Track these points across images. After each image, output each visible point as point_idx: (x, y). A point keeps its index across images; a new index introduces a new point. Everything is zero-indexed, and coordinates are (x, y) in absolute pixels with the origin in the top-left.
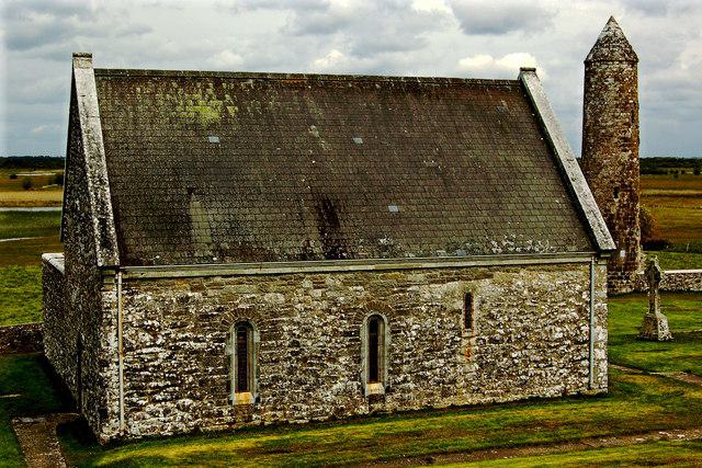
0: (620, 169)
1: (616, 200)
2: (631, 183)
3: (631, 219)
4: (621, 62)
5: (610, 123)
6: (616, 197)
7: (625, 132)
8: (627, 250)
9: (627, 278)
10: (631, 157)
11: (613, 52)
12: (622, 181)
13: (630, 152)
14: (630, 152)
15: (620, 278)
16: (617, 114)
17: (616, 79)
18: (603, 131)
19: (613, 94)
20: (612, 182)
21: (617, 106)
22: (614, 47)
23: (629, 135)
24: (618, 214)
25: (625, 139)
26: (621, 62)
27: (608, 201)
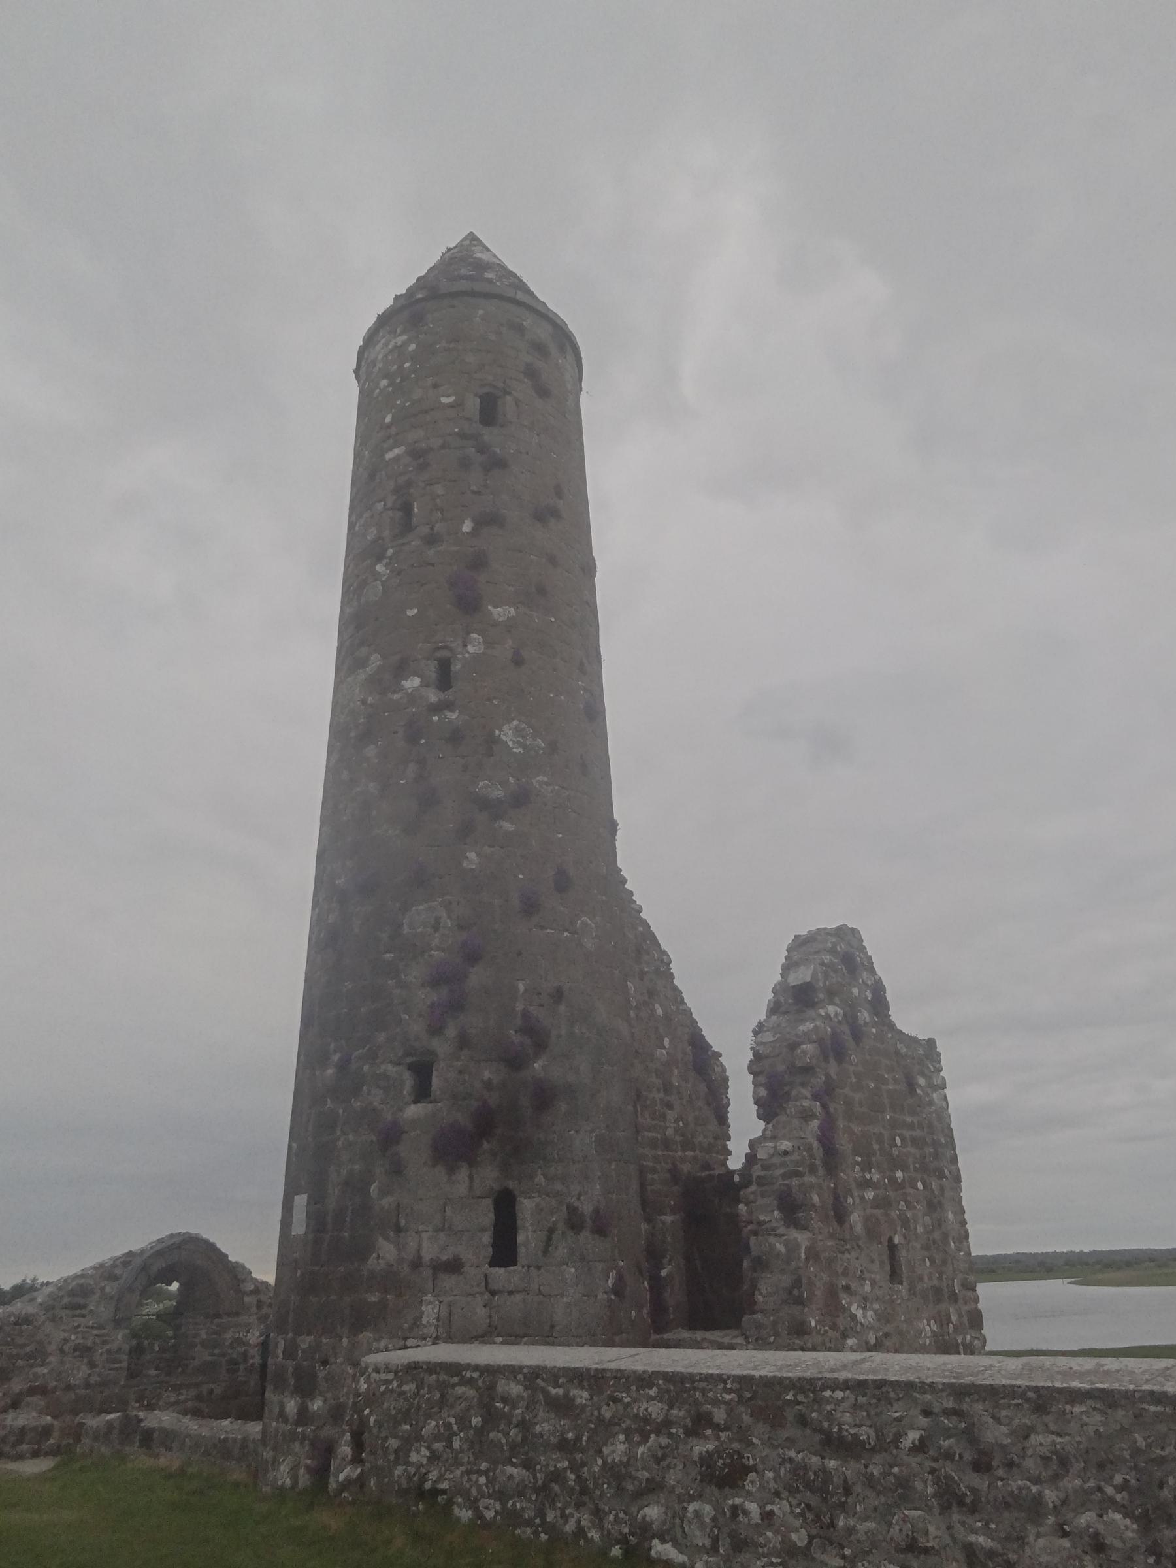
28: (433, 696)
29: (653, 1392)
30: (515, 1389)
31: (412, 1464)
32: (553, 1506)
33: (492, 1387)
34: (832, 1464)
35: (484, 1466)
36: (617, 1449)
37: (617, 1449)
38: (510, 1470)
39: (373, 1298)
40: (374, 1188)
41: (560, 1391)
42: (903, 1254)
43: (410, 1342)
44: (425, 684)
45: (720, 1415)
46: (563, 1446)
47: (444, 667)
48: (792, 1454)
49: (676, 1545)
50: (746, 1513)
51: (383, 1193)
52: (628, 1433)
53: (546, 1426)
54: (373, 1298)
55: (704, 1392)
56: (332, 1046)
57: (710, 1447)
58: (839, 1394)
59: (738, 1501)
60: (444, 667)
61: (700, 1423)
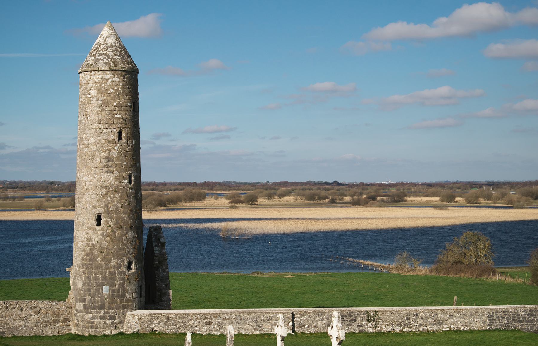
0: (104, 191)
1: (99, 228)
2: (117, 208)
5: (92, 141)
7: (110, 150)
8: (111, 285)
9: (112, 318)
10: (116, 178)
11: (98, 60)
12: (106, 206)
14: (116, 174)
15: (101, 318)
16: (100, 131)
17: (99, 91)
18: (86, 150)
19: (96, 109)
20: (95, 207)
21: (100, 121)
22: (100, 55)
24: (101, 245)
27: (90, 228)
29: (198, 315)
30: (173, 316)
31: (151, 327)
32: (180, 330)
33: (169, 316)
34: (223, 321)
35: (166, 326)
36: (192, 322)
37: (192, 322)
38: (172, 326)
39: (126, 304)
40: (125, 285)
41: (182, 316)
43: (132, 310)
45: (209, 317)
46: (183, 322)
48: (218, 321)
49: (201, 331)
50: (211, 327)
51: (127, 287)
52: (194, 320)
53: (180, 320)
54: (126, 304)
55: (206, 315)
56: (112, 258)
57: (207, 321)
58: (226, 314)
59: (210, 326)
61: (206, 318)
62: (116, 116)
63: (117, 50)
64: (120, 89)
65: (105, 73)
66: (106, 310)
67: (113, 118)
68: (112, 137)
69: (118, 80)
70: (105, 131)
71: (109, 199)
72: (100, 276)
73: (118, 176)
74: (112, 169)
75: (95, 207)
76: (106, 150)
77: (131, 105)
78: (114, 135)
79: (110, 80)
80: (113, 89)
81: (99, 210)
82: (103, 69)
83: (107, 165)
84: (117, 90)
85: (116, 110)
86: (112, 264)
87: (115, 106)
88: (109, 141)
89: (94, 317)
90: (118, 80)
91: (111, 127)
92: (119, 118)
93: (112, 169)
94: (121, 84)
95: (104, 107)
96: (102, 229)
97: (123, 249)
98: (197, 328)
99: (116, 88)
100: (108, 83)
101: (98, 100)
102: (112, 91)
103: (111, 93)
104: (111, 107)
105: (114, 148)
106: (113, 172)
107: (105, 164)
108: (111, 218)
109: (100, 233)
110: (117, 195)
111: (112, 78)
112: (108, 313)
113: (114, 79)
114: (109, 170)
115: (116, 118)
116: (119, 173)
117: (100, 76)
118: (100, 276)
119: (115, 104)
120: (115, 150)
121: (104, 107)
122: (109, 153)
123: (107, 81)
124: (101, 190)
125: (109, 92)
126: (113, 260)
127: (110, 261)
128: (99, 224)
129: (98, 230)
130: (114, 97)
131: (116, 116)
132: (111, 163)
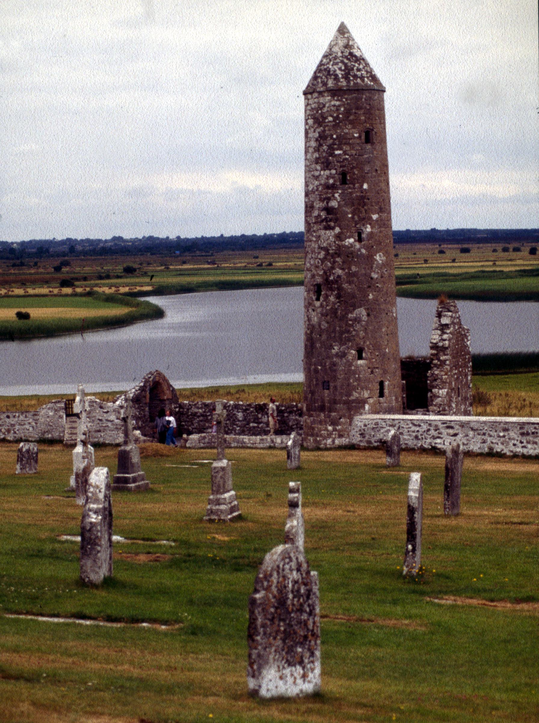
0: (322, 255)
1: (318, 304)
2: (339, 277)
3: (342, 333)
4: (320, 93)
6: (318, 299)
7: (328, 199)
10: (339, 237)
13: (337, 230)
14: (337, 230)
16: (317, 173)
21: (317, 161)
23: (334, 204)
24: (320, 325)
25: (329, 210)
26: (320, 93)
28: (358, 245)
42: (460, 391)
44: (355, 241)
47: (360, 235)
60: (360, 235)
62: (337, 152)
63: (342, 62)
64: (341, 116)
65: (322, 94)
66: (327, 413)
67: (332, 155)
68: (331, 181)
69: (337, 103)
70: (322, 172)
71: (329, 264)
72: (320, 368)
73: (340, 233)
74: (332, 224)
75: (313, 276)
76: (325, 199)
77: (360, 137)
78: (333, 178)
79: (327, 105)
80: (332, 116)
81: (319, 280)
82: (318, 90)
83: (326, 218)
84: (338, 117)
85: (336, 144)
86: (333, 351)
87: (335, 139)
88: (327, 187)
89: (313, 422)
90: (337, 103)
91: (329, 167)
92: (340, 155)
93: (332, 224)
94: (342, 109)
95: (322, 142)
96: (322, 306)
97: (348, 332)
98: (438, 441)
99: (335, 115)
100: (325, 110)
101: (314, 131)
102: (330, 119)
103: (329, 122)
104: (330, 142)
105: (333, 196)
106: (333, 228)
107: (324, 217)
108: (332, 290)
109: (319, 310)
110: (338, 259)
111: (330, 101)
112: (329, 416)
113: (333, 103)
114: (329, 226)
115: (336, 155)
116: (341, 229)
117: (316, 100)
118: (320, 368)
119: (335, 136)
120: (335, 199)
121: (322, 142)
122: (327, 203)
123: (324, 106)
124: (319, 253)
125: (327, 121)
126: (335, 346)
127: (331, 347)
128: (318, 299)
129: (316, 306)
130: (334, 126)
131: (337, 152)
132: (330, 216)
